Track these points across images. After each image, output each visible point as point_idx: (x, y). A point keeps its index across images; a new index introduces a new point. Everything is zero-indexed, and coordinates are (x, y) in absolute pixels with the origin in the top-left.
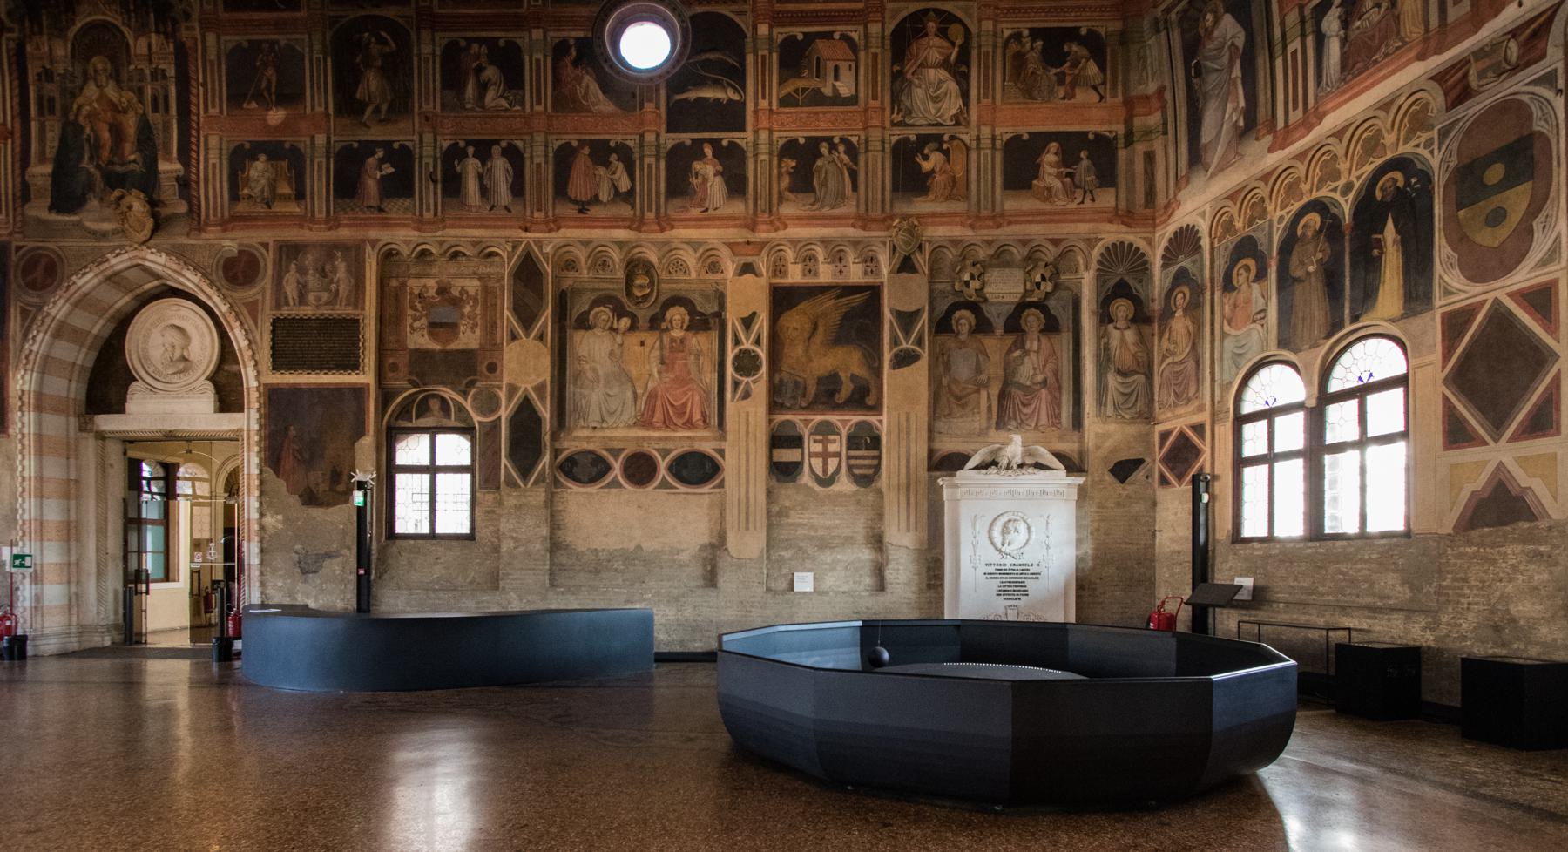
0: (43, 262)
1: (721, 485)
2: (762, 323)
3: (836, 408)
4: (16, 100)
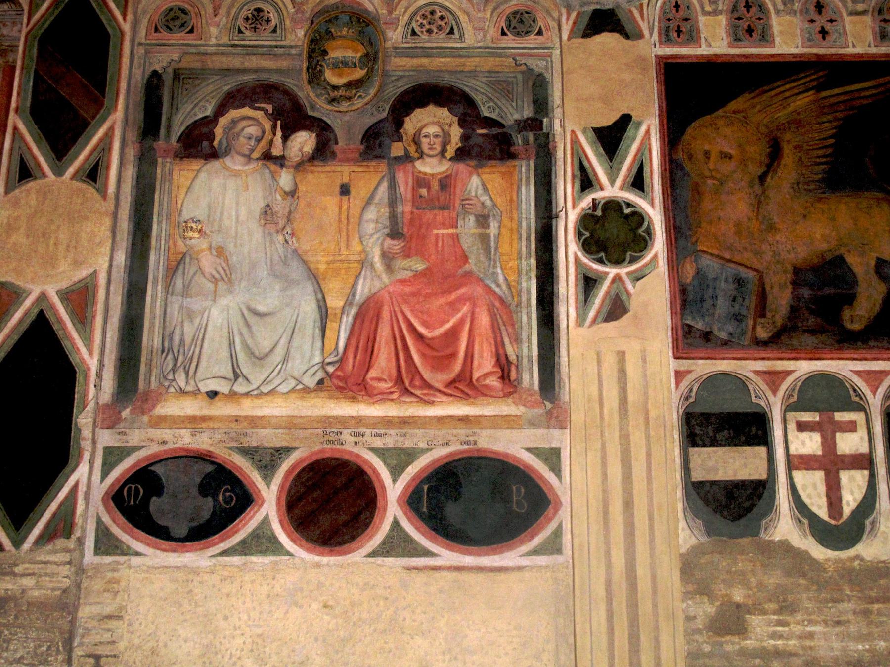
1: (553, 546)
2: (647, 137)
3: (848, 341)
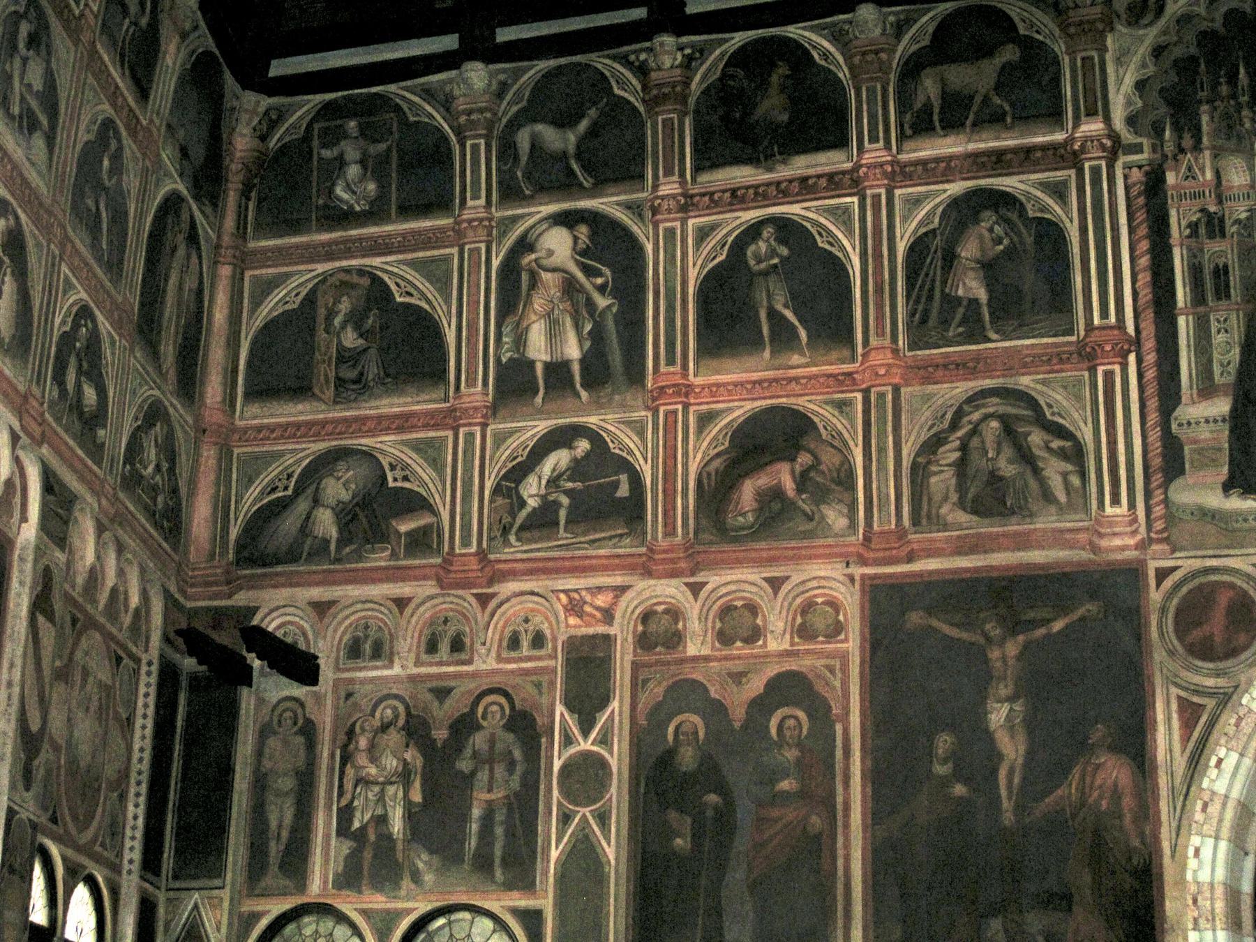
0: (1223, 600)
4: (1145, 278)
